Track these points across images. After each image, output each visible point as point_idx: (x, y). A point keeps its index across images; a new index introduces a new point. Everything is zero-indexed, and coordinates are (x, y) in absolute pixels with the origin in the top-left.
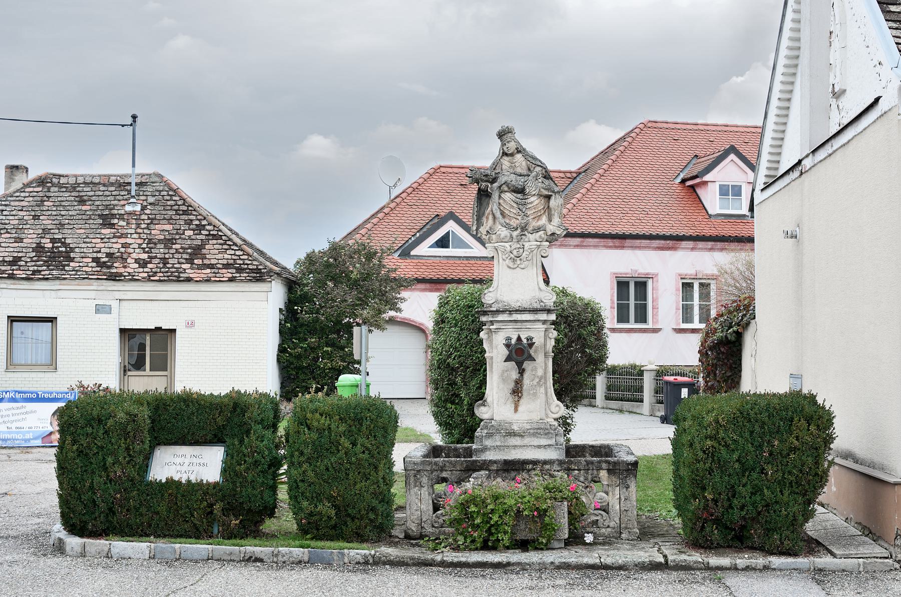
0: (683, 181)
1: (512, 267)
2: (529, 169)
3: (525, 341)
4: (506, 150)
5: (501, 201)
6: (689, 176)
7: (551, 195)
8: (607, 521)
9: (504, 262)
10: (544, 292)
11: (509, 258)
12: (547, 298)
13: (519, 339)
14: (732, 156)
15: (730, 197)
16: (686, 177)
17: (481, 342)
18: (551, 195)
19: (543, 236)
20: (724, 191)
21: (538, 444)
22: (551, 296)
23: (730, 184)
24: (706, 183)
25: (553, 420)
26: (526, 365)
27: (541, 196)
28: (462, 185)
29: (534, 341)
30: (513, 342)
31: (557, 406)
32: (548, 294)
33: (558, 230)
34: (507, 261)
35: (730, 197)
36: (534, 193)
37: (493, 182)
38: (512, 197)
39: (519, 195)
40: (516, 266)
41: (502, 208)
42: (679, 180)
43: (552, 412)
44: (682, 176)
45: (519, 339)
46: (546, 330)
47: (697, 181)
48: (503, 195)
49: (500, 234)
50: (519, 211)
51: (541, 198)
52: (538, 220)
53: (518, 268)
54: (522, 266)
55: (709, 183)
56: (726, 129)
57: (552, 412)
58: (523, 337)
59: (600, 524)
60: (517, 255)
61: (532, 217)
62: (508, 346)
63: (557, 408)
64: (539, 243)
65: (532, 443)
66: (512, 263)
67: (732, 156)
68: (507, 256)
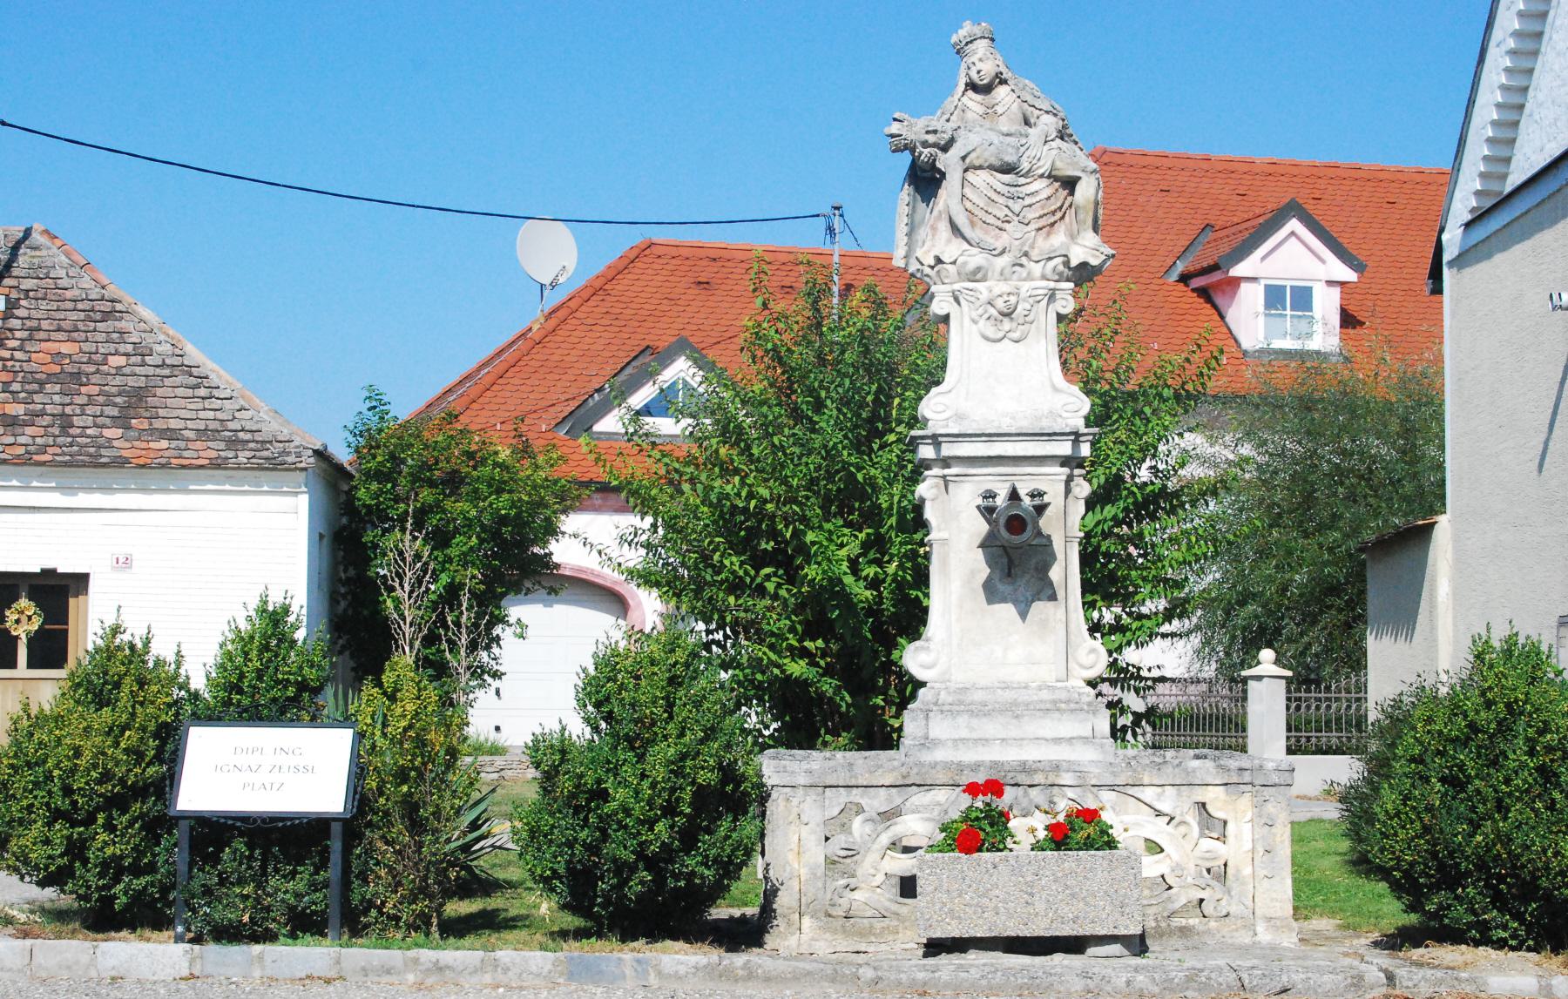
0: (1184, 278)
1: (992, 336)
2: (1027, 122)
3: (1027, 501)
5: (967, 191)
6: (1198, 267)
7: (1079, 178)
8: (1223, 903)
9: (974, 326)
11: (986, 316)
12: (1070, 407)
13: (1014, 496)
14: (1294, 224)
15: (1288, 312)
16: (1192, 269)
17: (918, 508)
19: (1061, 268)
20: (1274, 296)
23: (1289, 284)
24: (1236, 282)
25: (1084, 684)
27: (1056, 179)
29: (1046, 499)
30: (1001, 501)
31: (1093, 651)
32: (1072, 399)
33: (1094, 256)
34: (982, 322)
35: (1288, 312)
36: (1041, 171)
37: (945, 148)
39: (1007, 178)
40: (1000, 335)
41: (968, 205)
42: (1174, 276)
43: (1083, 667)
44: (1180, 267)
45: (1014, 496)
46: (1069, 480)
47: (1216, 277)
48: (970, 176)
49: (965, 263)
50: (1007, 211)
51: (1057, 184)
52: (1049, 234)
53: (1006, 340)
54: (1015, 335)
55: (1244, 286)
56: (1274, 171)
58: (1022, 492)
59: (1208, 908)
60: (1005, 310)
61: (1037, 226)
62: (988, 512)
63: (1092, 657)
64: (1052, 285)
66: (993, 329)
67: (1294, 224)
68: (981, 311)
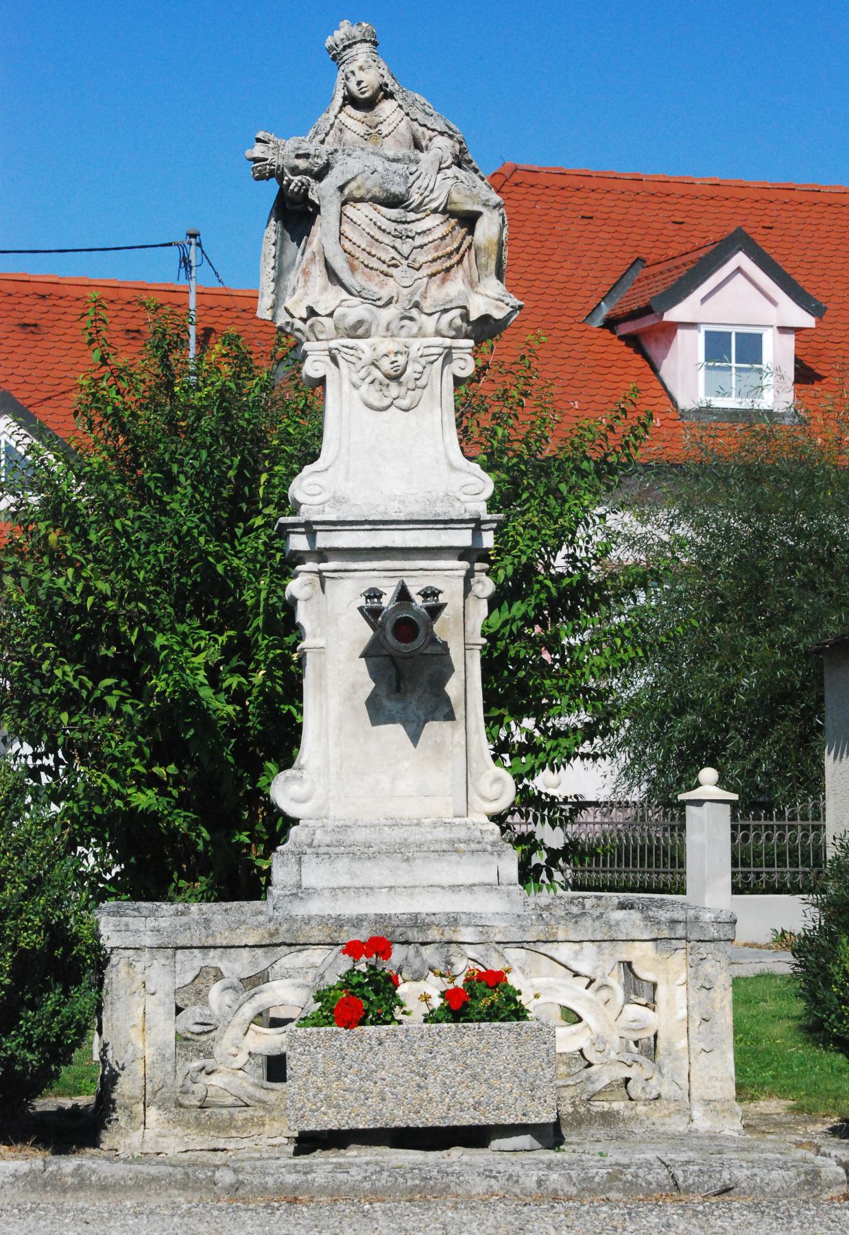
0: (610, 324)
1: (377, 404)
2: (417, 145)
3: (419, 601)
4: (354, 88)
5: (346, 228)
6: (627, 309)
7: (479, 214)
8: (653, 1082)
9: (355, 392)
10: (463, 475)
11: (369, 379)
12: (469, 489)
13: (403, 595)
14: (740, 259)
15: (733, 364)
16: (619, 312)
17: (290, 607)
18: (479, 214)
19: (458, 322)
20: (717, 346)
21: (452, 881)
22: (480, 485)
23: (734, 330)
24: (673, 327)
25: (486, 820)
26: (496, 612)
27: (453, 214)
28: (25, 325)
29: (442, 599)
30: (387, 602)
31: (497, 780)
32: (472, 479)
33: (497, 307)
34: (364, 387)
35: (733, 364)
36: (434, 205)
37: (320, 176)
38: (374, 215)
39: (394, 213)
40: (387, 402)
41: (348, 245)
42: (598, 321)
43: (484, 798)
44: (605, 310)
45: (403, 595)
46: (469, 575)
47: (648, 322)
48: (349, 210)
49: (344, 316)
50: (394, 253)
51: (453, 221)
52: (443, 281)
53: (393, 408)
54: (404, 403)
55: (681, 333)
56: (717, 194)
57: (484, 798)
58: (413, 591)
59: (635, 1089)
60: (392, 372)
61: (429, 271)
62: (371, 614)
63: (497, 788)
64: (448, 342)
65: (436, 879)
66: (377, 395)
67: (740, 259)
68: (363, 373)
